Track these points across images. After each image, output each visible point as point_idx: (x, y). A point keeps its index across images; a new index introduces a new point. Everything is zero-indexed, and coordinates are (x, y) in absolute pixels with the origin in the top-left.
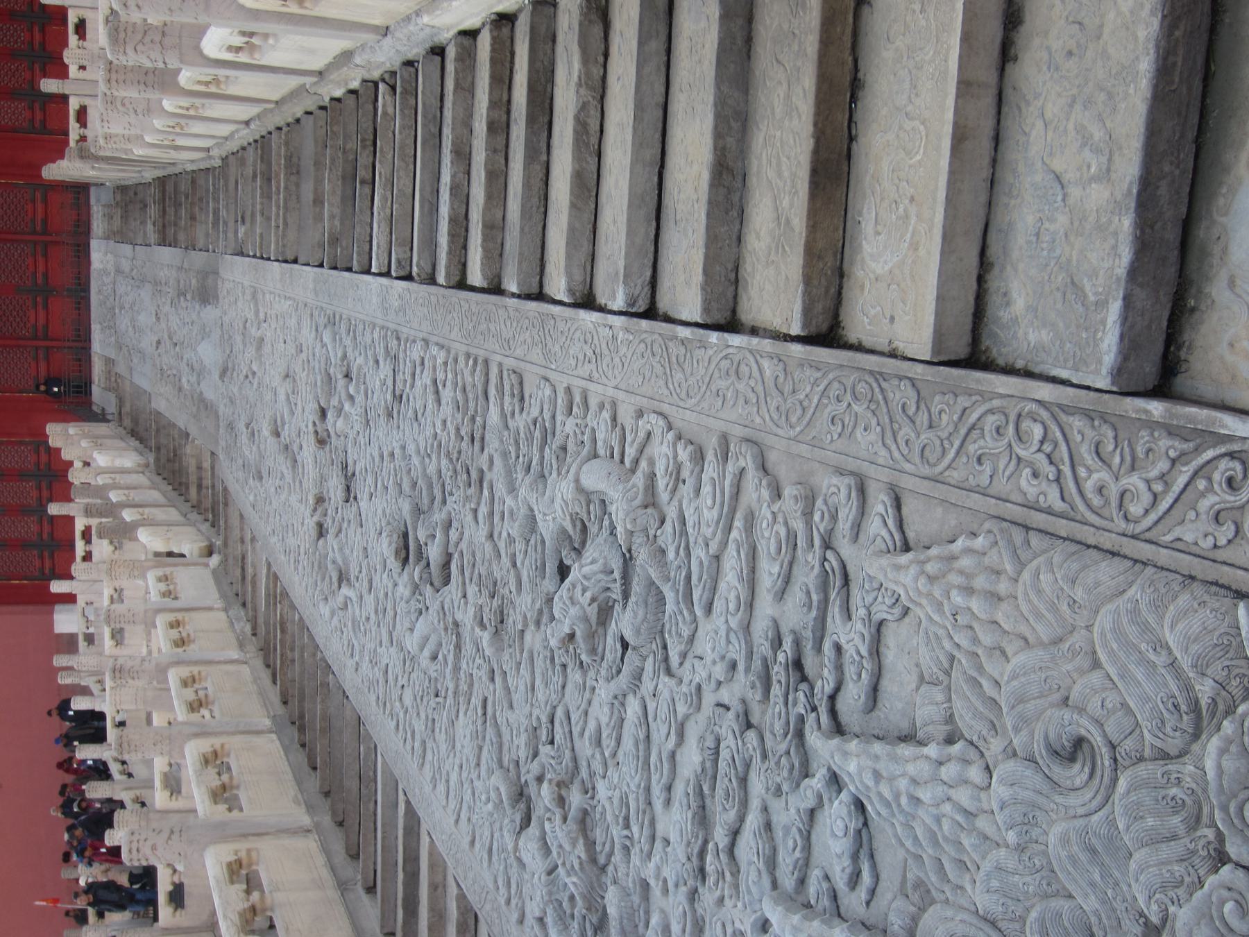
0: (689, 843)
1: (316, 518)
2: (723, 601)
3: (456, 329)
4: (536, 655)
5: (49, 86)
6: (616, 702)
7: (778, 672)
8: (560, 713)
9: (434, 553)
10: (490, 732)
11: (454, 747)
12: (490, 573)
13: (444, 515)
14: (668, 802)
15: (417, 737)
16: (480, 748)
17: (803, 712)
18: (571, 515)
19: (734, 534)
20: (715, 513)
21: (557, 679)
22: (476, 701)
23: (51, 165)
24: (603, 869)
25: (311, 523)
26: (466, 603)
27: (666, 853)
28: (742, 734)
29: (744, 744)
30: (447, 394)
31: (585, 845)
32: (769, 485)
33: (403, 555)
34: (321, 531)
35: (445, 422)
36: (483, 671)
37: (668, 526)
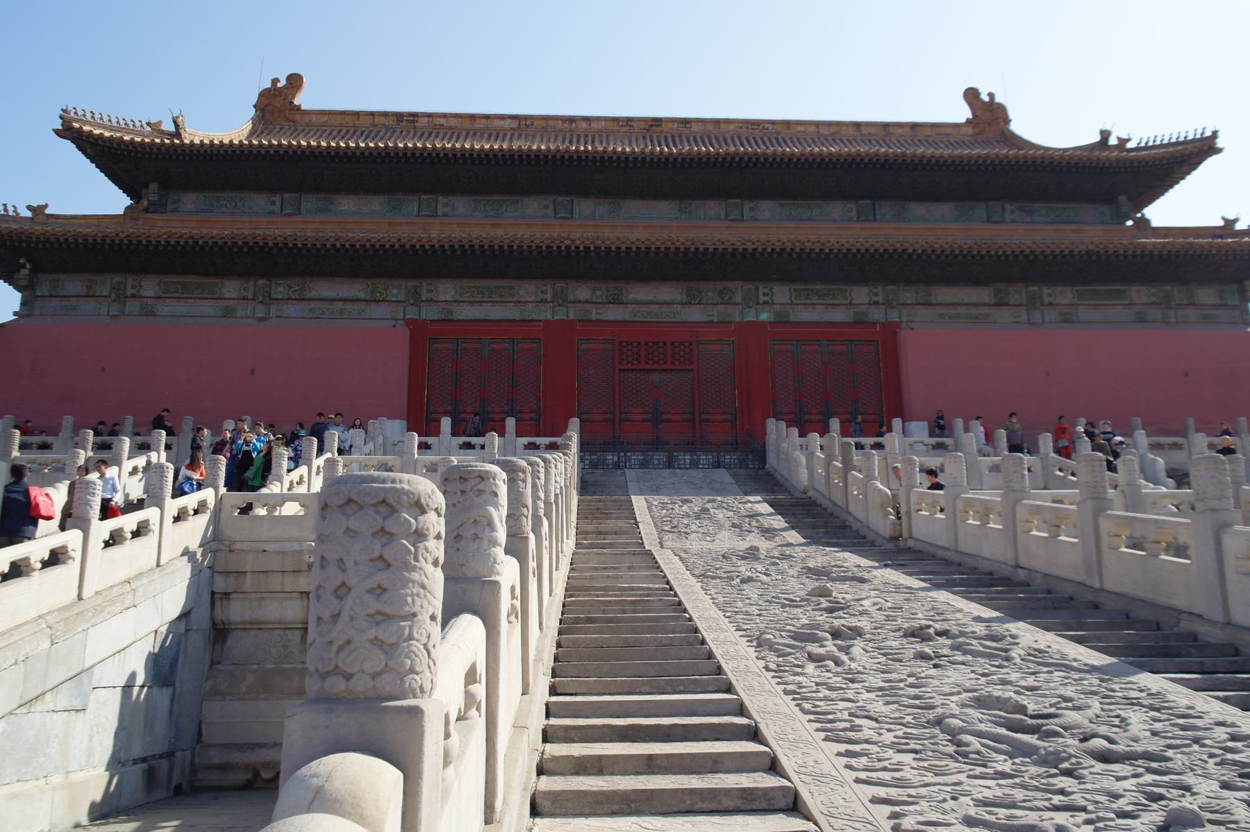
23: (783, 425)
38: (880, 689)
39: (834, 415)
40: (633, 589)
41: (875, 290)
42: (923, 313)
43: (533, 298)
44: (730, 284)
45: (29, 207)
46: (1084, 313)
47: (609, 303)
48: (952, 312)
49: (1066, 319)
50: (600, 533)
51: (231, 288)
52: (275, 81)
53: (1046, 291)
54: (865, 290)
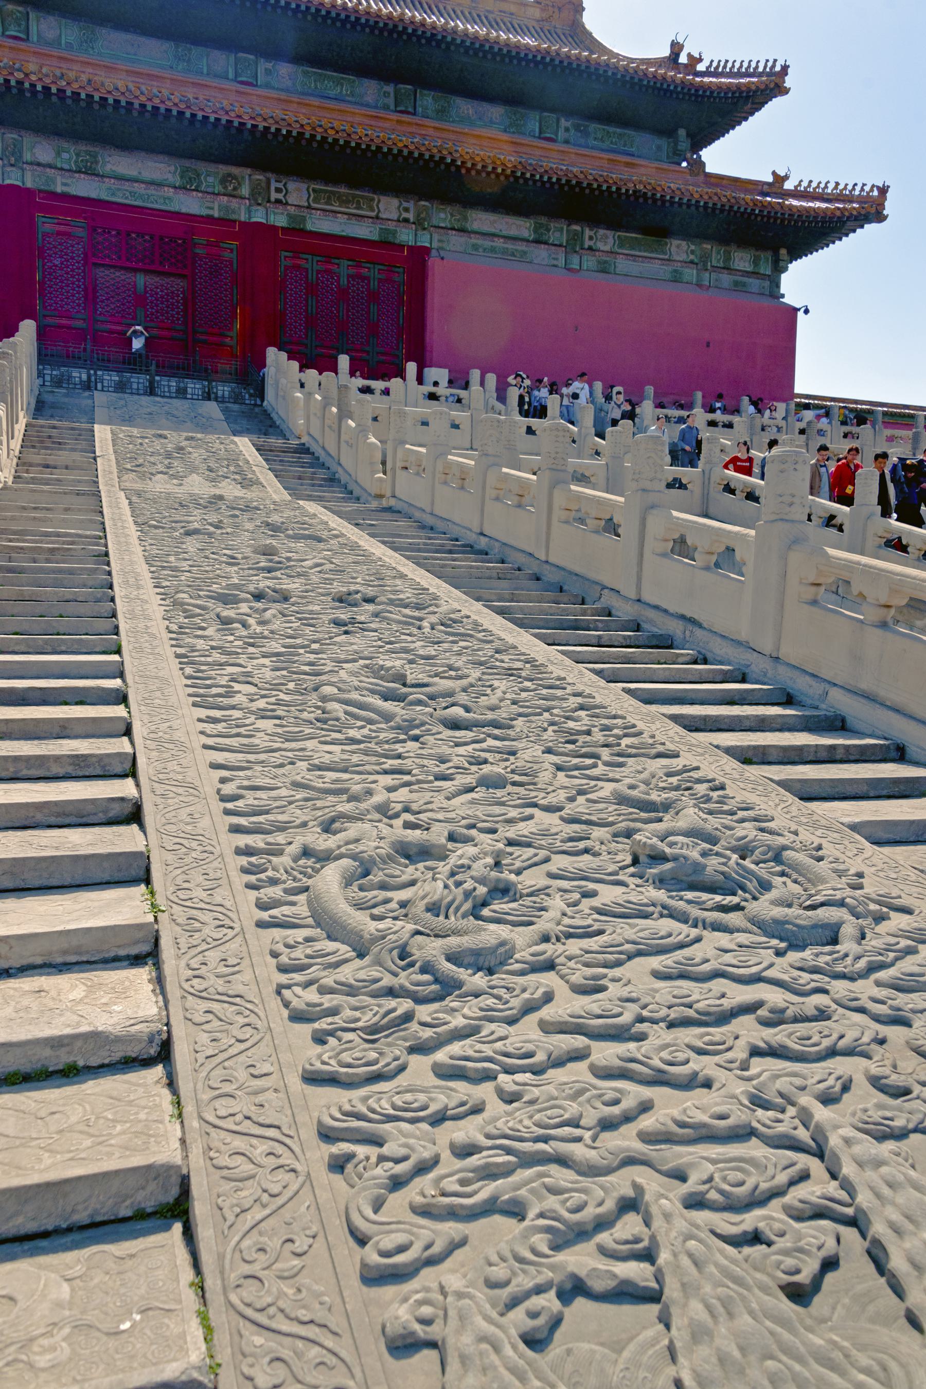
6: (659, 908)
23: (284, 355)
38: (277, 654)
40: (58, 535)
41: (405, 204)
42: (456, 241)
44: (236, 171)
46: (623, 265)
47: (80, 172)
48: (487, 243)
49: (604, 269)
50: (47, 466)
53: (588, 232)
54: (395, 202)
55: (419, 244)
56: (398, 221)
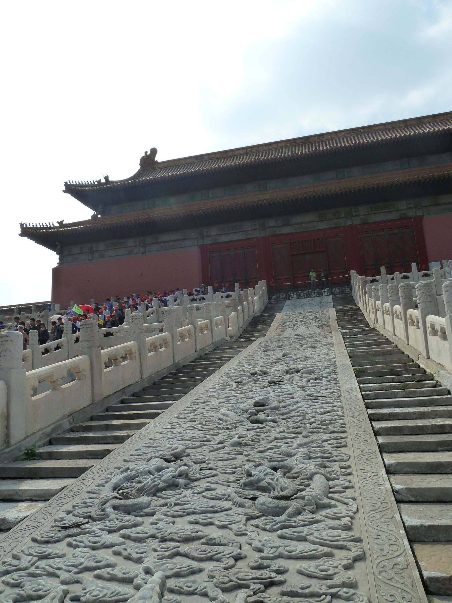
0: (177, 534)
1: (258, 372)
2: (289, 544)
3: (353, 419)
4: (235, 460)
5: (383, 269)
6: (227, 496)
7: (266, 574)
8: (215, 472)
9: (261, 416)
10: (199, 444)
11: (187, 429)
12: (262, 439)
13: (278, 419)
14: (191, 523)
15: (187, 415)
16: (190, 440)
17: (252, 588)
18: (300, 472)
19: (321, 548)
20: (326, 538)
21: (228, 471)
22: (209, 438)
24: (155, 495)
25: (256, 370)
26: (245, 431)
27: (169, 523)
28: (232, 557)
29: (228, 558)
30: (325, 417)
31: (164, 486)
32: (349, 564)
33: (256, 405)
34: (254, 374)
35: (314, 417)
36: (221, 439)
37: (311, 516)
39: (382, 265)
40: (221, 358)
43: (250, 229)
45: (58, 222)
47: (284, 226)
51: (130, 242)
52: (146, 153)
55: (418, 215)
56: (407, 209)
